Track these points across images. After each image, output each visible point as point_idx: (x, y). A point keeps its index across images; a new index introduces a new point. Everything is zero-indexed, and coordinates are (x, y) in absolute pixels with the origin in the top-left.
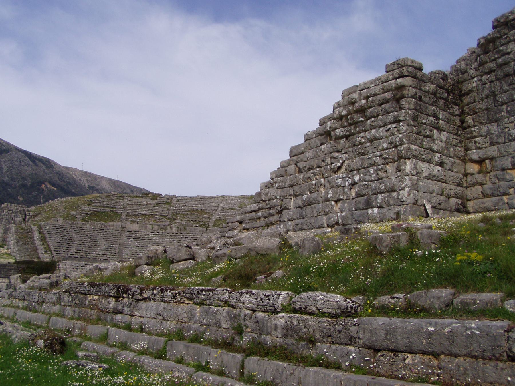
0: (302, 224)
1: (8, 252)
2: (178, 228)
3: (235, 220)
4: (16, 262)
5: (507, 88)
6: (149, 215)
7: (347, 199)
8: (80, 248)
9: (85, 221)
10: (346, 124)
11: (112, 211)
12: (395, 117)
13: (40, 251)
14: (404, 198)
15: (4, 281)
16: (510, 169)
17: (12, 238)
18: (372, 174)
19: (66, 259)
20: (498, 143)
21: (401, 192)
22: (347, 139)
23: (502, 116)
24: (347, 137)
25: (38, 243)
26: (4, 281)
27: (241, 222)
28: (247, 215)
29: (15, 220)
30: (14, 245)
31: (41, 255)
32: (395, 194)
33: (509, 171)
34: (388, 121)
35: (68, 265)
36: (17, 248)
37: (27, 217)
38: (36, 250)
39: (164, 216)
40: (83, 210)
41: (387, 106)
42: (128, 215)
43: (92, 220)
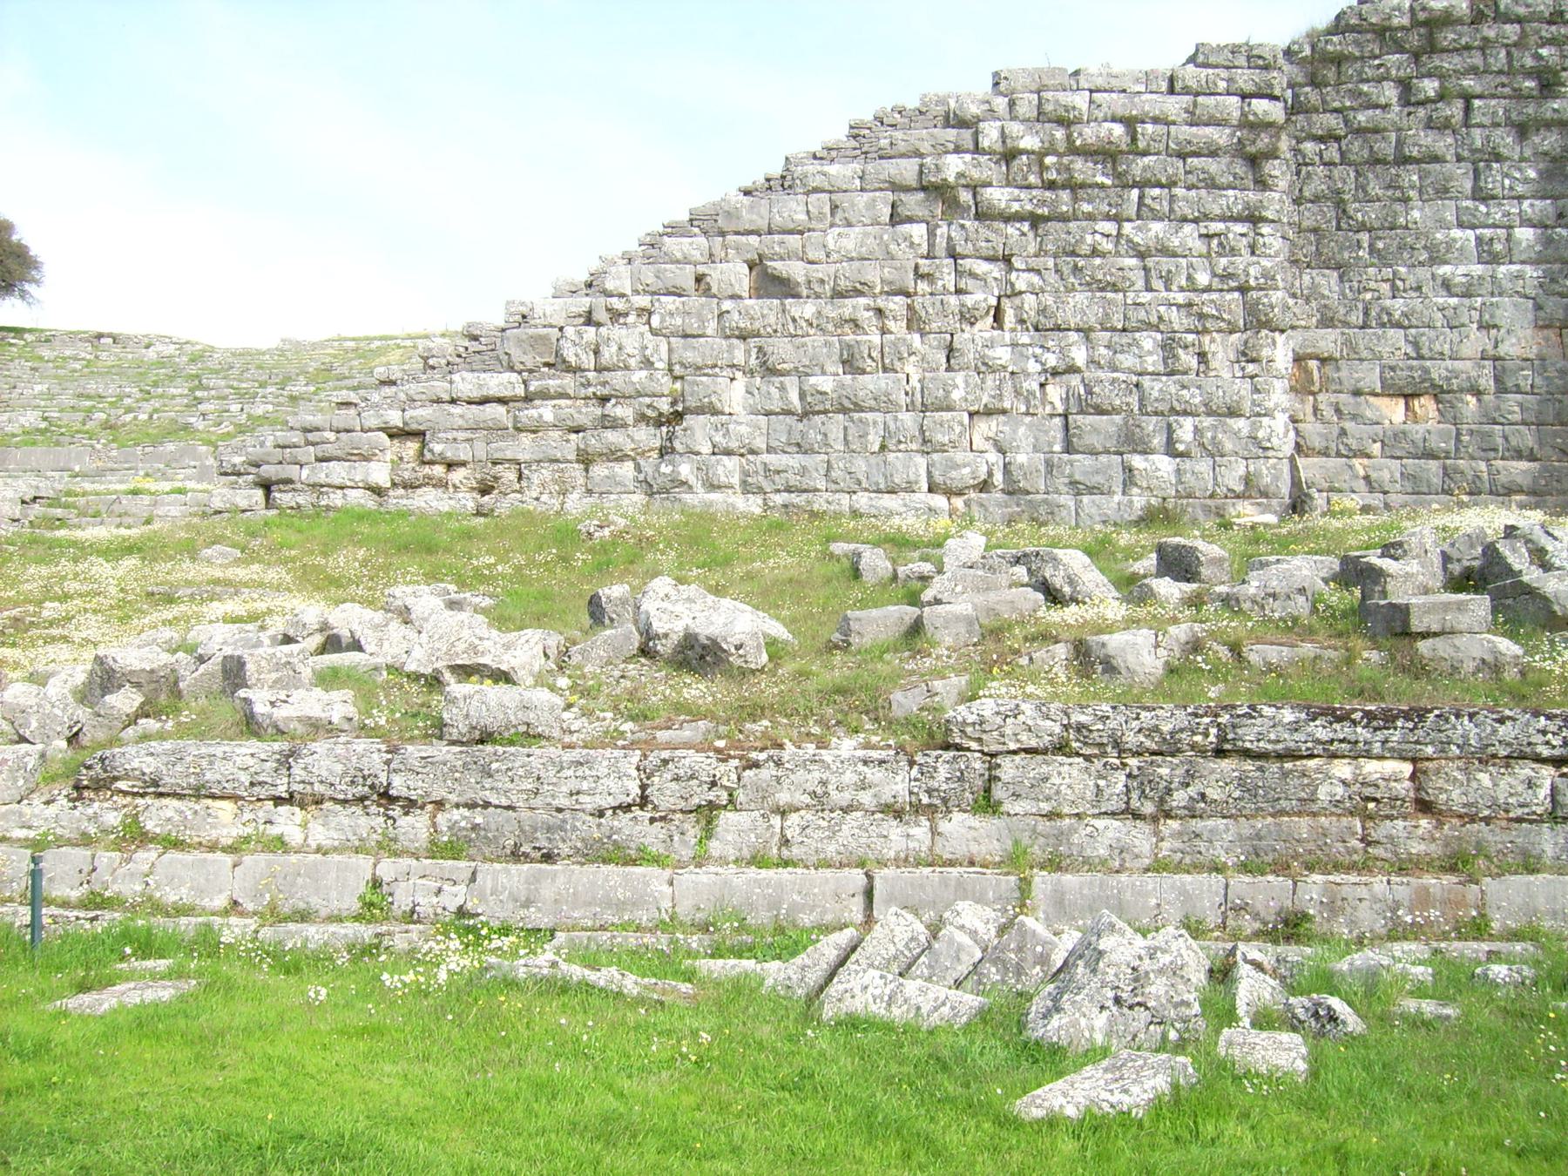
0: (804, 471)
3: (373, 422)
5: (1380, 192)
7: (1027, 414)
10: (1032, 179)
12: (1247, 206)
14: (1275, 441)
16: (1376, 395)
18: (1150, 353)
20: (1346, 324)
21: (1265, 420)
22: (1034, 226)
23: (1358, 258)
24: (1035, 221)
27: (398, 434)
28: (456, 410)
32: (1240, 424)
33: (1372, 399)
34: (1218, 212)
41: (1212, 166)
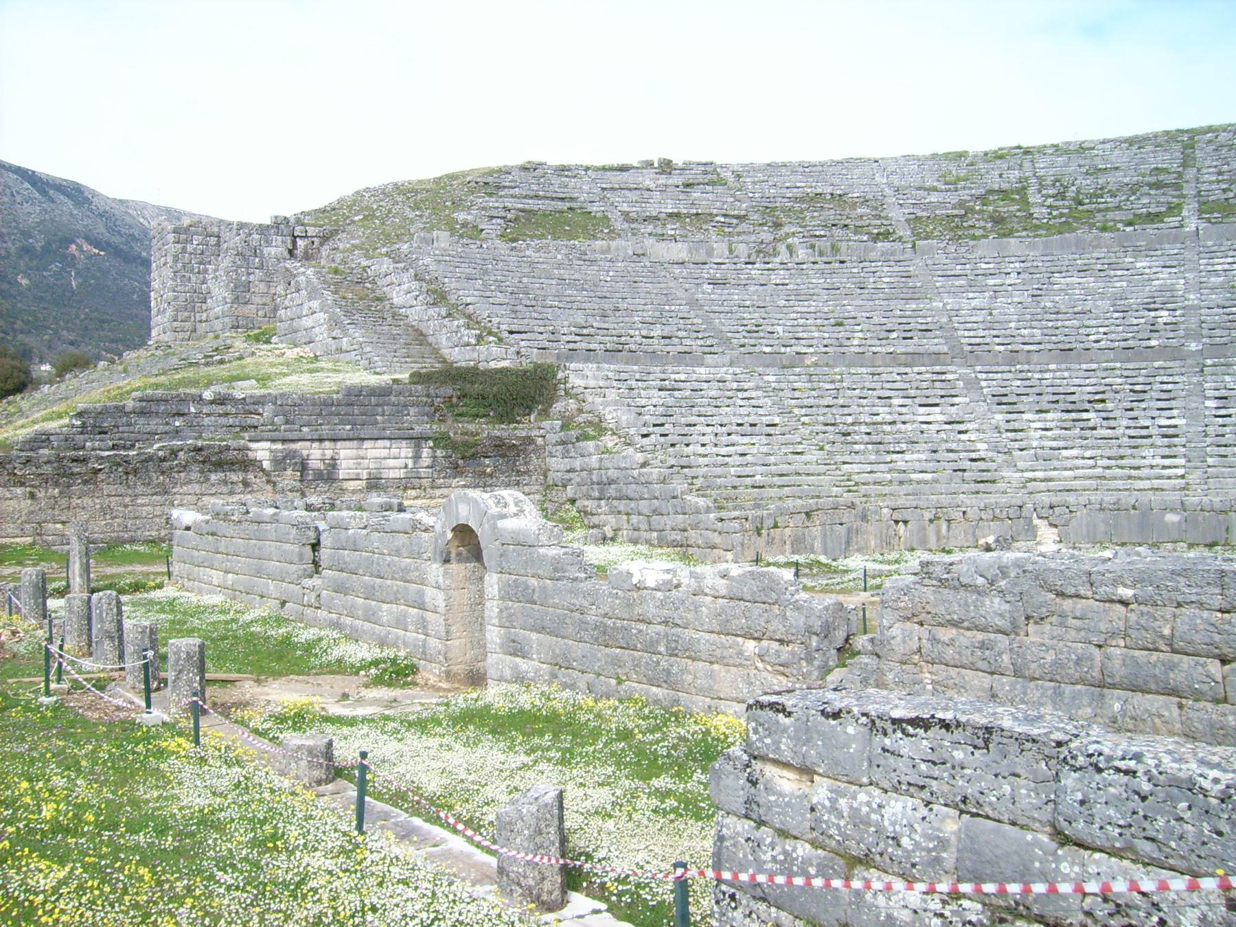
1: (307, 351)
2: (812, 247)
4: (417, 378)
6: (689, 216)
8: (580, 319)
9: (515, 240)
11: (570, 209)
13: (443, 341)
15: (394, 451)
17: (315, 304)
19: (569, 358)
25: (419, 313)
26: (394, 451)
29: (262, 257)
30: (334, 323)
31: (445, 352)
35: (595, 378)
36: (358, 334)
37: (300, 242)
38: (420, 337)
39: (737, 217)
40: (484, 209)
42: (626, 216)
43: (532, 237)
